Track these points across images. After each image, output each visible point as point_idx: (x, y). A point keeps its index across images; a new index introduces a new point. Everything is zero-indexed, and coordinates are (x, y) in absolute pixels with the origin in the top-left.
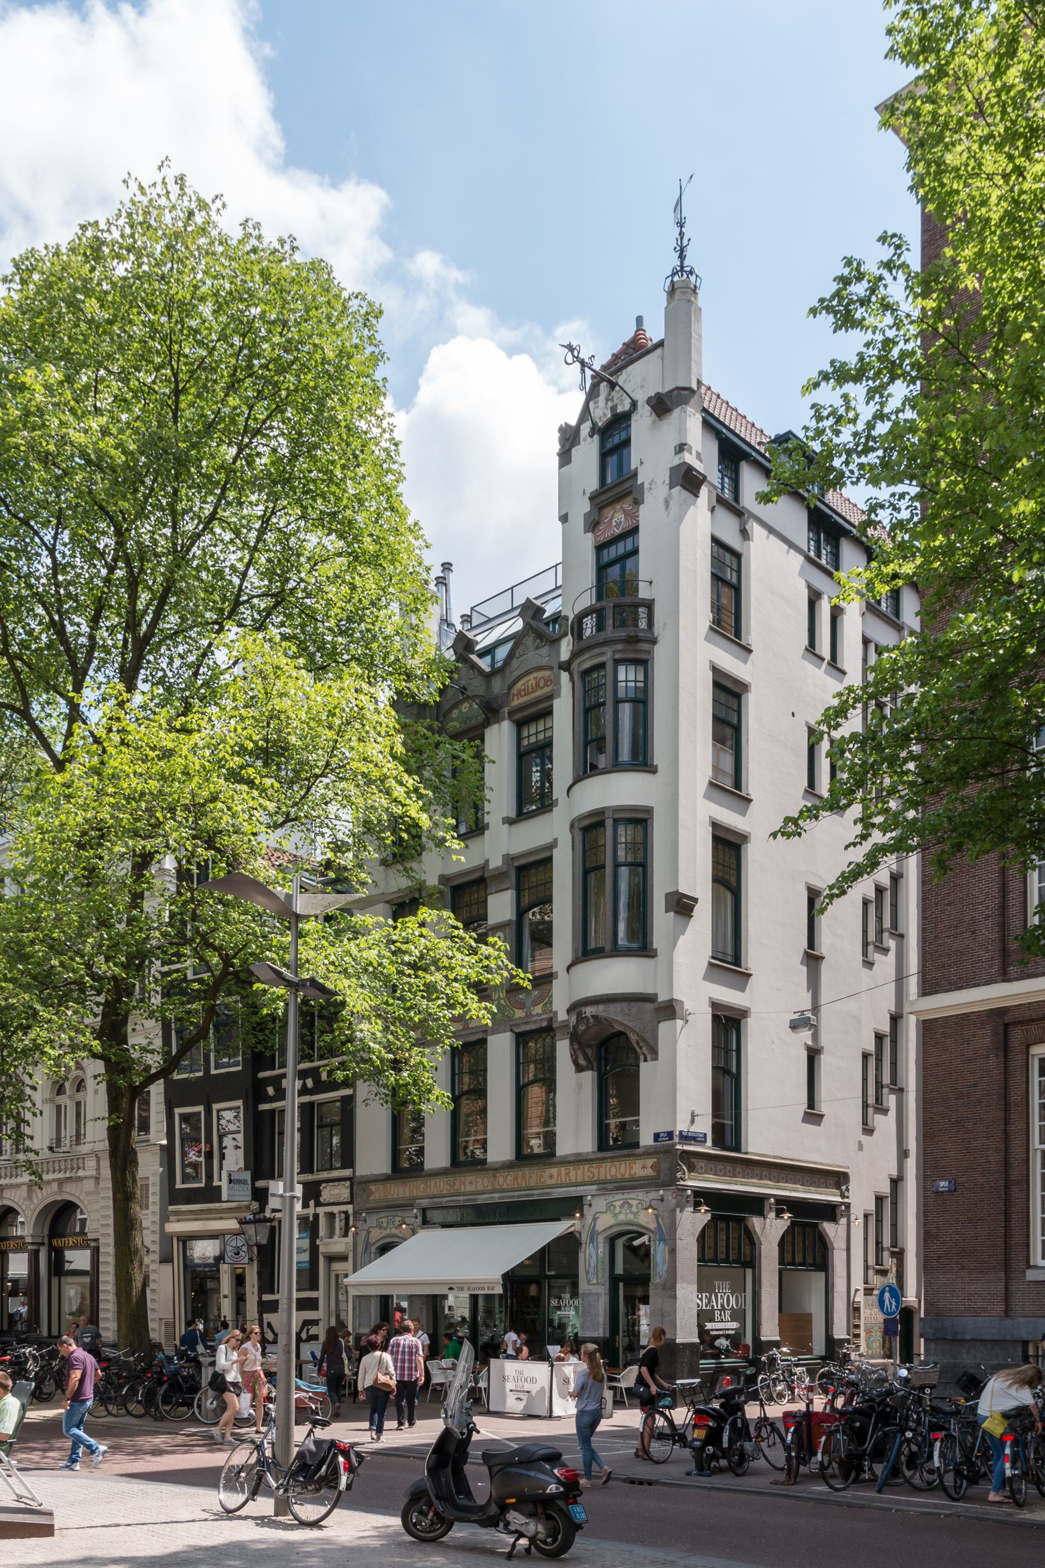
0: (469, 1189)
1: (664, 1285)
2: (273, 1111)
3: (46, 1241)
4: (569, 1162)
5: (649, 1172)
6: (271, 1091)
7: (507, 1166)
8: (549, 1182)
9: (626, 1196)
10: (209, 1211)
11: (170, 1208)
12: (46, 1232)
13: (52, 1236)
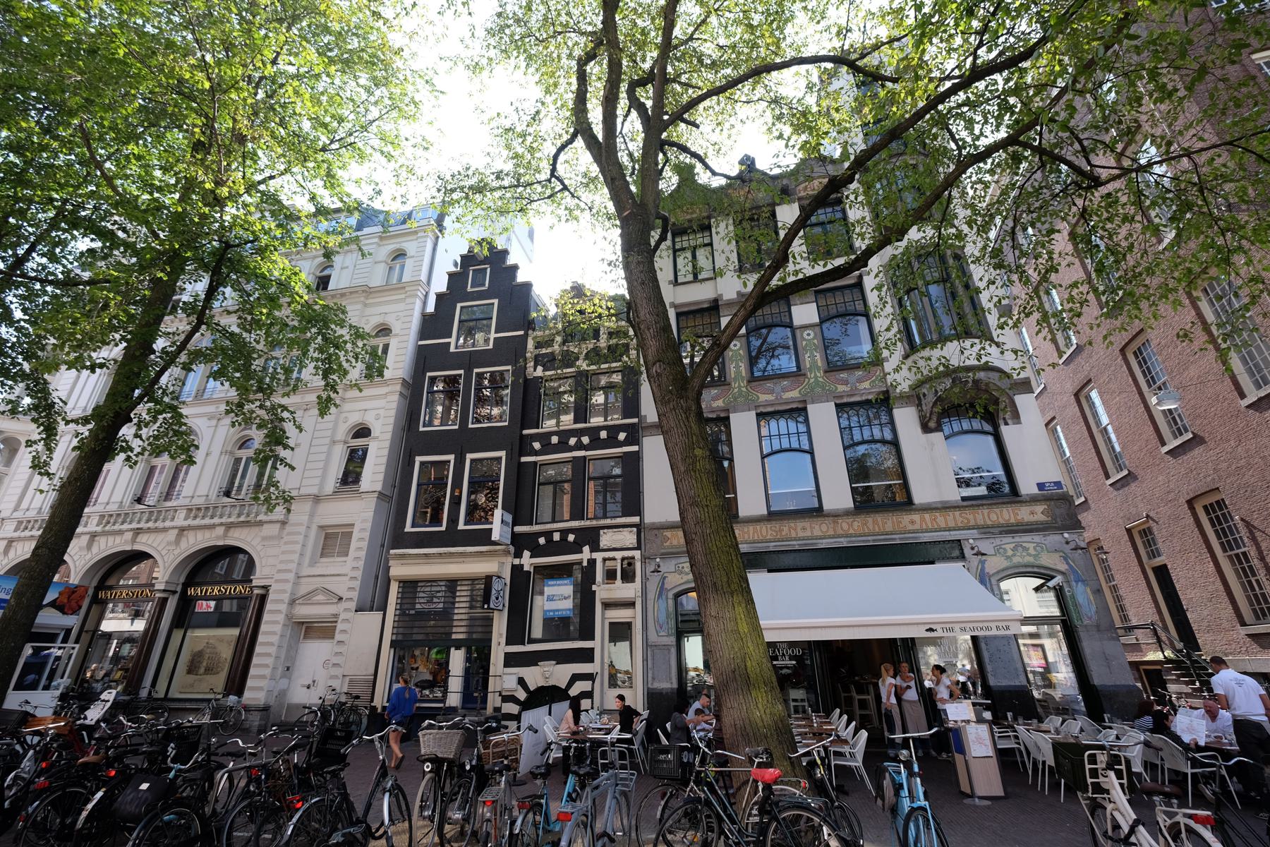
0: (801, 534)
1: (1098, 627)
2: (535, 463)
3: (179, 589)
4: (936, 509)
5: (1042, 518)
6: (537, 445)
7: (847, 513)
8: (911, 527)
9: (1017, 539)
10: (451, 554)
11: (392, 552)
12: (182, 580)
13: (186, 585)
